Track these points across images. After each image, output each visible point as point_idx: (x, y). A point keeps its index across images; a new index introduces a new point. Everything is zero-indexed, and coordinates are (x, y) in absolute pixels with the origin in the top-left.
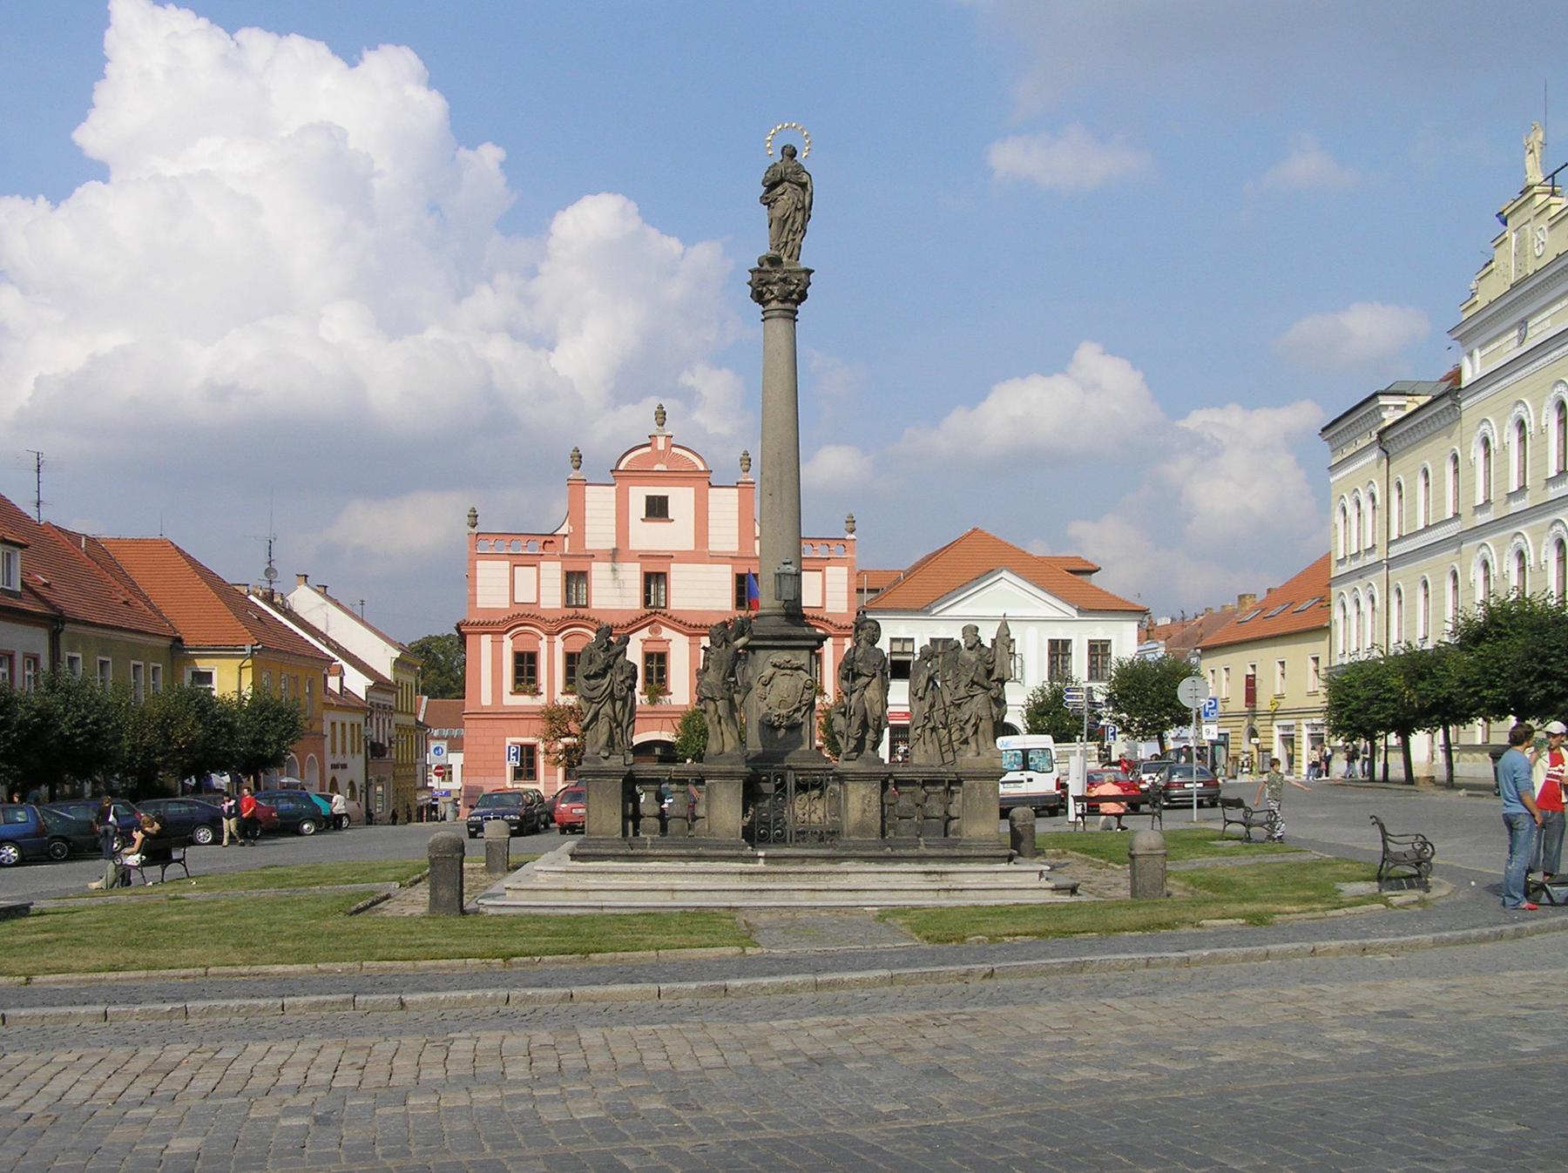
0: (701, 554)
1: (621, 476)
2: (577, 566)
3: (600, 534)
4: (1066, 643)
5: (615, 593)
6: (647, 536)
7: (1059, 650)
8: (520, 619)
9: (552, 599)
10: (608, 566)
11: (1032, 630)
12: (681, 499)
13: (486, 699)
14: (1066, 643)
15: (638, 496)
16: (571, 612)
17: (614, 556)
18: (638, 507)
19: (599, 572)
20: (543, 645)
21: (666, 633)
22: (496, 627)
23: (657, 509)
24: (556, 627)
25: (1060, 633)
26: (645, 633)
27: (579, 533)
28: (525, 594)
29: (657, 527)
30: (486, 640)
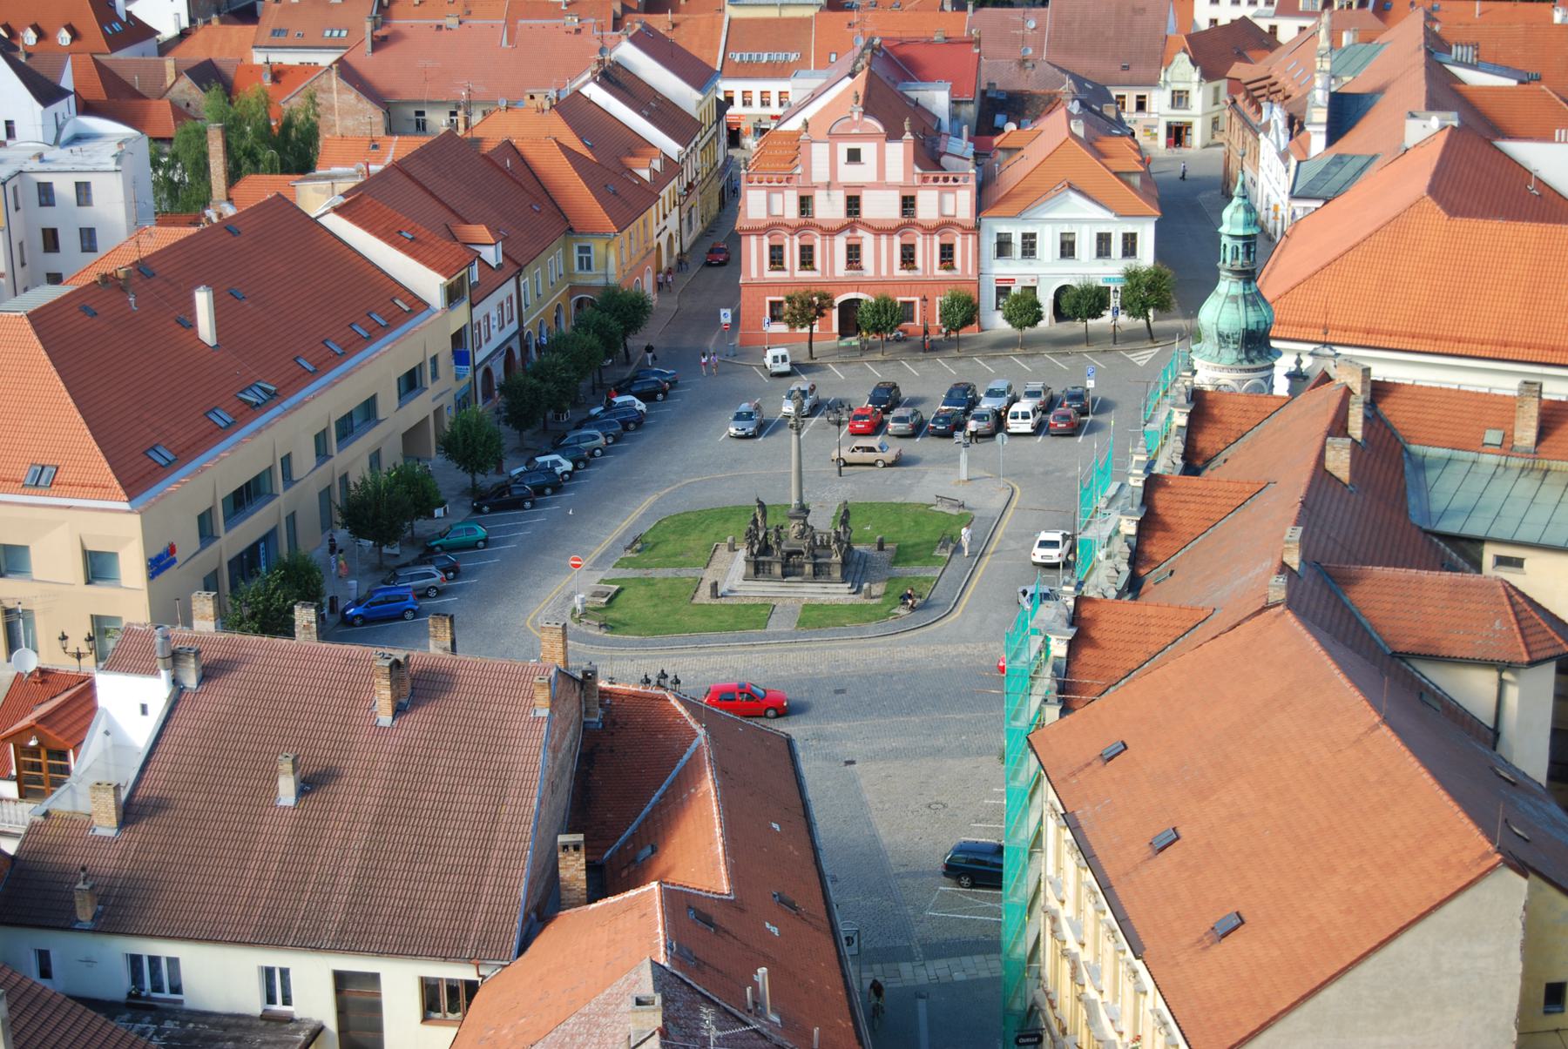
0: (882, 184)
1: (833, 137)
2: (805, 193)
3: (820, 172)
4: (1134, 236)
5: (829, 208)
6: (850, 174)
7: (1103, 241)
8: (772, 227)
9: (792, 212)
10: (824, 192)
11: (1086, 228)
12: (868, 150)
13: (754, 274)
14: (1134, 236)
15: (843, 149)
16: (802, 221)
17: (829, 186)
18: (842, 156)
19: (820, 198)
20: (787, 242)
21: (860, 233)
22: (759, 231)
23: (854, 156)
24: (796, 230)
25: (1104, 229)
26: (848, 233)
27: (808, 172)
28: (777, 211)
29: (854, 167)
30: (753, 239)
